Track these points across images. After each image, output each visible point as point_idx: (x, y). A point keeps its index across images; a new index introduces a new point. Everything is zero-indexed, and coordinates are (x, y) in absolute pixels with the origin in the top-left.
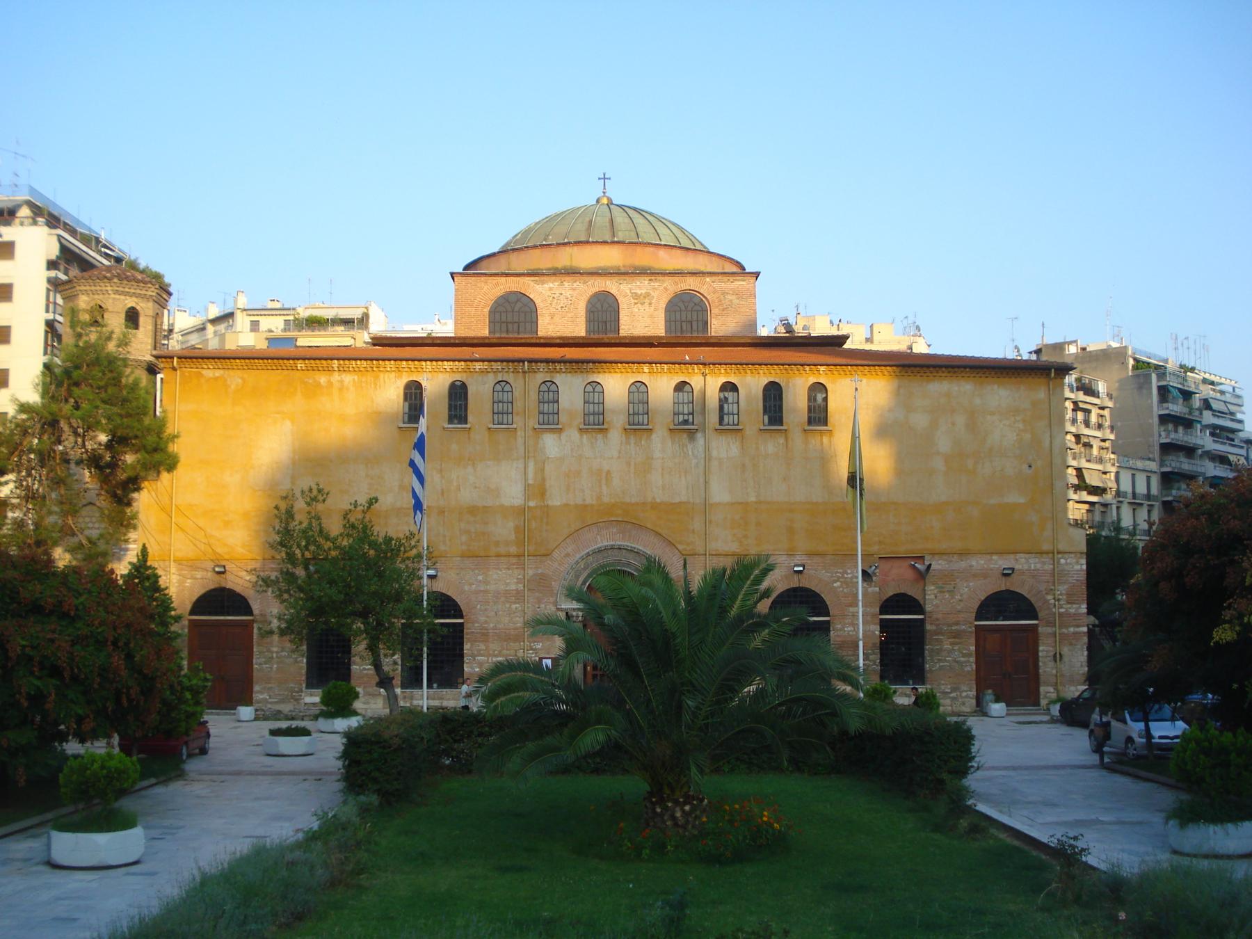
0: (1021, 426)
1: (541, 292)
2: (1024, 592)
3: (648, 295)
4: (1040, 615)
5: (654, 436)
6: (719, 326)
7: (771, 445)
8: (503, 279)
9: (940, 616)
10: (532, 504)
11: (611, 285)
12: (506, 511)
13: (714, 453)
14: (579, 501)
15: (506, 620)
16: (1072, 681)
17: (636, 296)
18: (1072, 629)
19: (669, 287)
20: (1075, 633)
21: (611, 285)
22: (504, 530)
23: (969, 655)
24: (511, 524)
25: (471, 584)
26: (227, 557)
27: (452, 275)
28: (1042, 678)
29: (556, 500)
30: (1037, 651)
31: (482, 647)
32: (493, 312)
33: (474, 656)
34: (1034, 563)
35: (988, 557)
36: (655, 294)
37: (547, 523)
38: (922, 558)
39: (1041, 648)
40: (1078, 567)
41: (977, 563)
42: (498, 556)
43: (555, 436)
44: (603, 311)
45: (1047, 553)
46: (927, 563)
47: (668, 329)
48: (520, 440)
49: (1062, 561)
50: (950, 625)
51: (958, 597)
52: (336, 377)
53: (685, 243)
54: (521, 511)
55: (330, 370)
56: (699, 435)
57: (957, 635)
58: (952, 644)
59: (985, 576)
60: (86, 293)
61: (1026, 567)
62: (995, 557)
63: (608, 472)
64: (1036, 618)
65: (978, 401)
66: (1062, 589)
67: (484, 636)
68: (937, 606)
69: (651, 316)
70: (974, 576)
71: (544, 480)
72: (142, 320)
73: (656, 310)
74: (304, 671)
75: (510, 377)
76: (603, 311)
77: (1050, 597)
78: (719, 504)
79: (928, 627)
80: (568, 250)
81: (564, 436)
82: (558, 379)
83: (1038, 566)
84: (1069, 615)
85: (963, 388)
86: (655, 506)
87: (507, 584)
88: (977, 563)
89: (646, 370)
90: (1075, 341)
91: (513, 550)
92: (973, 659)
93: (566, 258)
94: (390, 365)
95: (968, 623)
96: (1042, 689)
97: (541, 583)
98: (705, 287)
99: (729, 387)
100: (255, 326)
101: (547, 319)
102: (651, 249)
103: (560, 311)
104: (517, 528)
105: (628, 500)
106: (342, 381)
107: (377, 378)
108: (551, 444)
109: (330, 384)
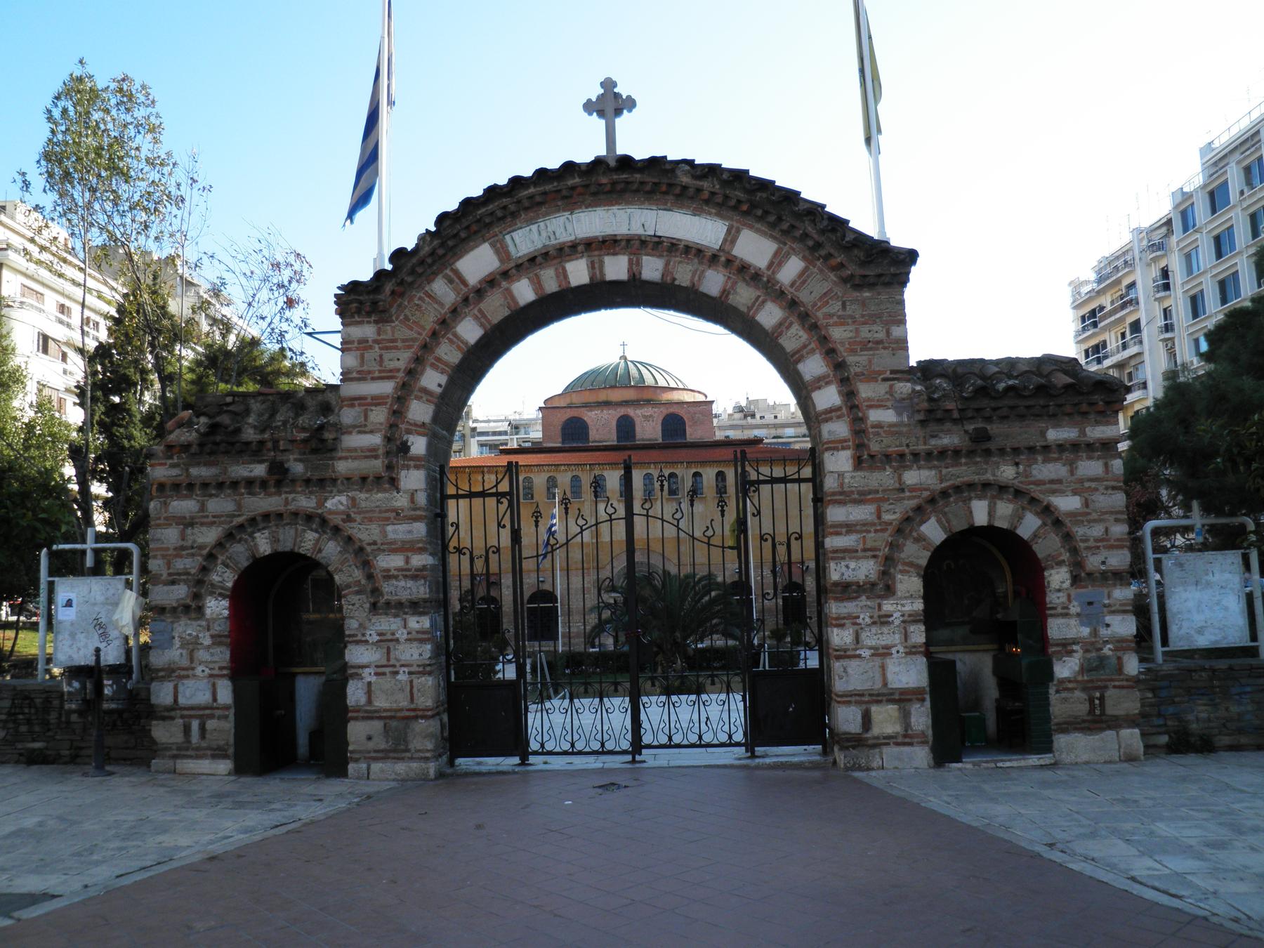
1: (590, 417)
6: (693, 434)
11: (631, 411)
19: (665, 411)
21: (631, 411)
32: (564, 429)
44: (626, 427)
47: (663, 436)
53: (673, 385)
75: (580, 474)
76: (626, 427)
82: (605, 473)
93: (603, 396)
98: (681, 412)
99: (696, 475)
103: (602, 426)
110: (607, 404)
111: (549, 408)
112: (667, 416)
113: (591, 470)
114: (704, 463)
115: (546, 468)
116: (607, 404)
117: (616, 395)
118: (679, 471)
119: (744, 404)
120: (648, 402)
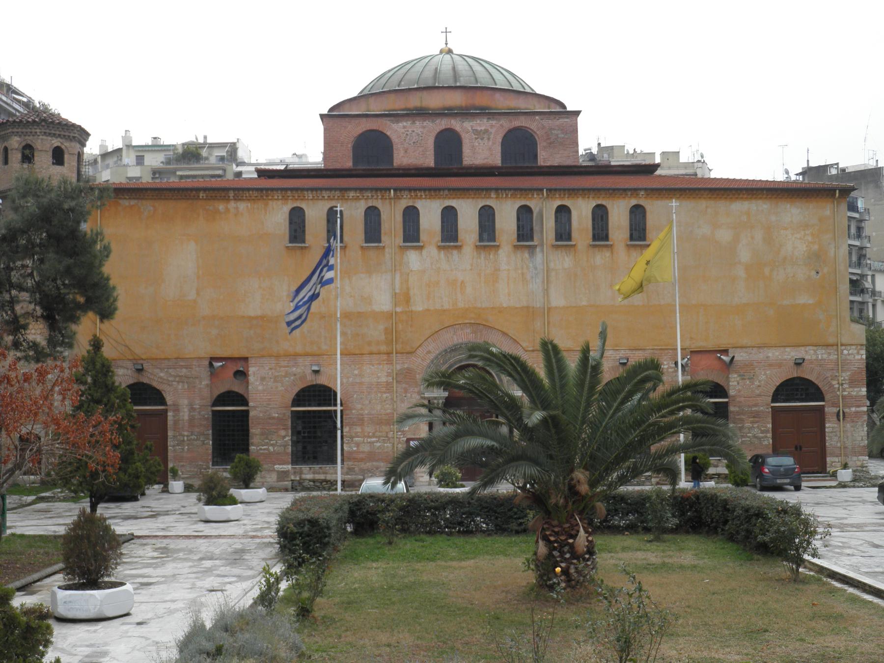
0: (810, 238)
1: (396, 131)
2: (812, 378)
3: (486, 131)
4: (827, 397)
5: (501, 251)
6: (546, 157)
7: (600, 258)
8: (364, 120)
9: (742, 399)
10: (399, 310)
11: (456, 124)
12: (377, 316)
13: (552, 265)
14: (438, 307)
15: (379, 407)
16: (855, 453)
17: (476, 132)
18: (853, 409)
19: (507, 124)
20: (857, 412)
21: (456, 124)
22: (376, 332)
23: (767, 432)
24: (381, 327)
25: (348, 378)
26: (144, 357)
27: (322, 116)
28: (828, 451)
29: (418, 306)
30: (824, 427)
31: (359, 429)
33: (352, 438)
34: (822, 354)
35: (782, 349)
36: (493, 131)
37: (411, 326)
38: (725, 352)
39: (827, 425)
40: (859, 357)
41: (774, 354)
42: (371, 353)
43: (417, 252)
44: (448, 144)
45: (832, 345)
46: (731, 355)
48: (387, 256)
49: (845, 352)
50: (749, 406)
51: (757, 383)
52: (232, 205)
54: (389, 315)
55: (227, 199)
56: (538, 249)
57: (756, 415)
58: (752, 422)
59: (780, 365)
60: (17, 134)
61: (814, 357)
62: (788, 349)
63: (462, 282)
64: (823, 400)
65: (773, 218)
66: (846, 375)
67: (361, 421)
68: (739, 391)
69: (490, 149)
70: (771, 365)
71: (408, 289)
72: (66, 156)
73: (494, 143)
74: (210, 451)
75: (378, 204)
76: (448, 144)
77: (834, 382)
78: (556, 308)
79: (732, 408)
80: (419, 94)
81: (424, 252)
82: (420, 204)
83: (825, 356)
84: (851, 397)
85: (760, 207)
86: (501, 310)
87: (378, 377)
88: (774, 354)
89: (493, 195)
90: (837, 164)
91: (383, 348)
92: (770, 435)
93: (415, 101)
94: (277, 195)
95: (765, 404)
96: (829, 460)
97: (406, 376)
98: (532, 125)
100: (140, 160)
101: (402, 153)
102: (489, 92)
103: (413, 144)
104: (386, 329)
105: (479, 305)
106: (237, 208)
107: (266, 205)
108: (413, 258)
109: (227, 210)
110: (421, 113)
111: (334, 118)
112: (510, 131)
113: (397, 198)
114: (573, 192)
115: (326, 194)
116: (421, 113)
117: (434, 101)
118: (534, 203)
119: (595, 151)
120: (485, 112)
